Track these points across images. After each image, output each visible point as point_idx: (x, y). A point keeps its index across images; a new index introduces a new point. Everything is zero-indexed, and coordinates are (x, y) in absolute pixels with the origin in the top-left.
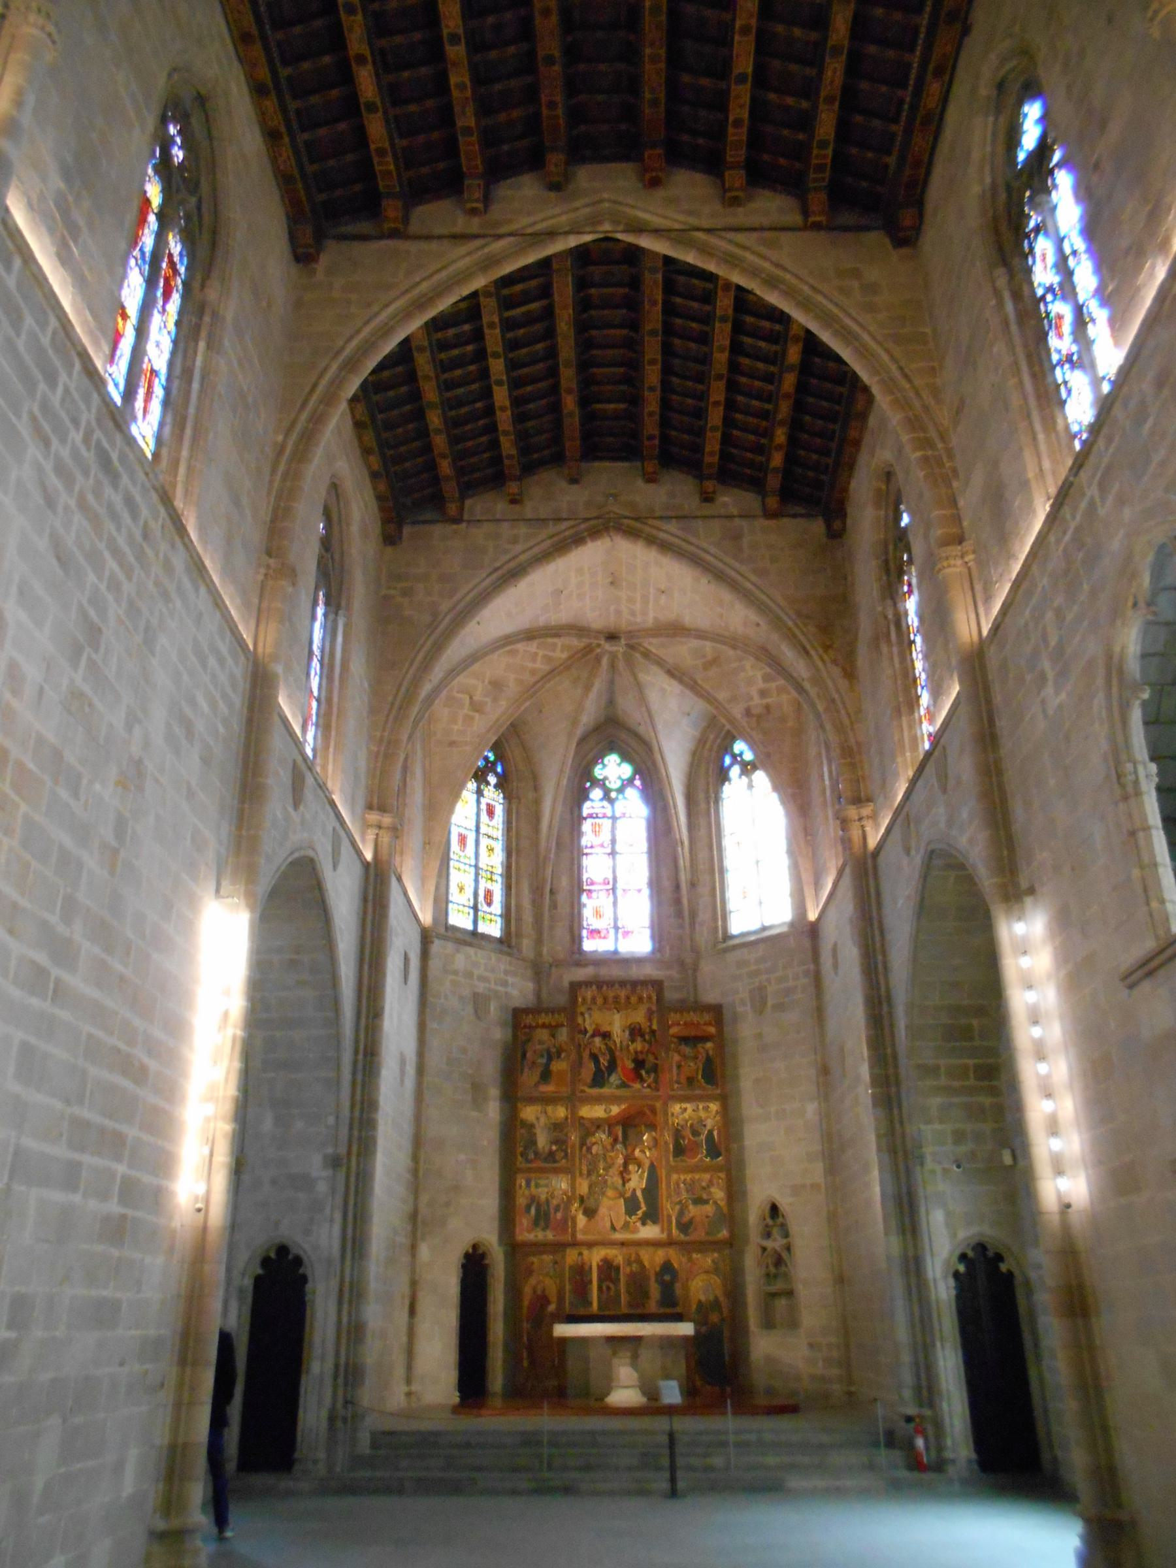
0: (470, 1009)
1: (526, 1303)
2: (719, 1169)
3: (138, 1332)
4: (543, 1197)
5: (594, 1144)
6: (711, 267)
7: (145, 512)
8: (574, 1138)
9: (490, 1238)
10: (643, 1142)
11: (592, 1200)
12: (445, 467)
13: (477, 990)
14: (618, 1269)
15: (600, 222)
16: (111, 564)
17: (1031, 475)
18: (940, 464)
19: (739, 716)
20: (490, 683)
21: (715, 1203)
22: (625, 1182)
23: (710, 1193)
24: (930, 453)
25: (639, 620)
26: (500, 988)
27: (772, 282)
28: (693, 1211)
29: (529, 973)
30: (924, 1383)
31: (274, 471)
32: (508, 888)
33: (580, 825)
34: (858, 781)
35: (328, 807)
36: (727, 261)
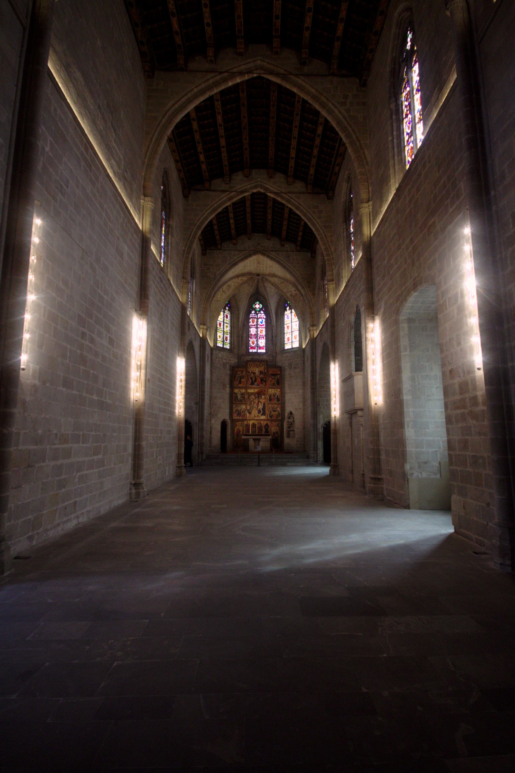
0: (222, 366)
1: (235, 432)
2: (280, 404)
4: (239, 409)
6: (284, 202)
8: (246, 397)
9: (227, 418)
10: (262, 398)
12: (218, 237)
14: (256, 425)
17: (343, 276)
19: (289, 296)
21: (278, 411)
23: (277, 409)
24: (329, 257)
25: (265, 271)
27: (297, 208)
28: (273, 413)
32: (231, 337)
34: (313, 321)
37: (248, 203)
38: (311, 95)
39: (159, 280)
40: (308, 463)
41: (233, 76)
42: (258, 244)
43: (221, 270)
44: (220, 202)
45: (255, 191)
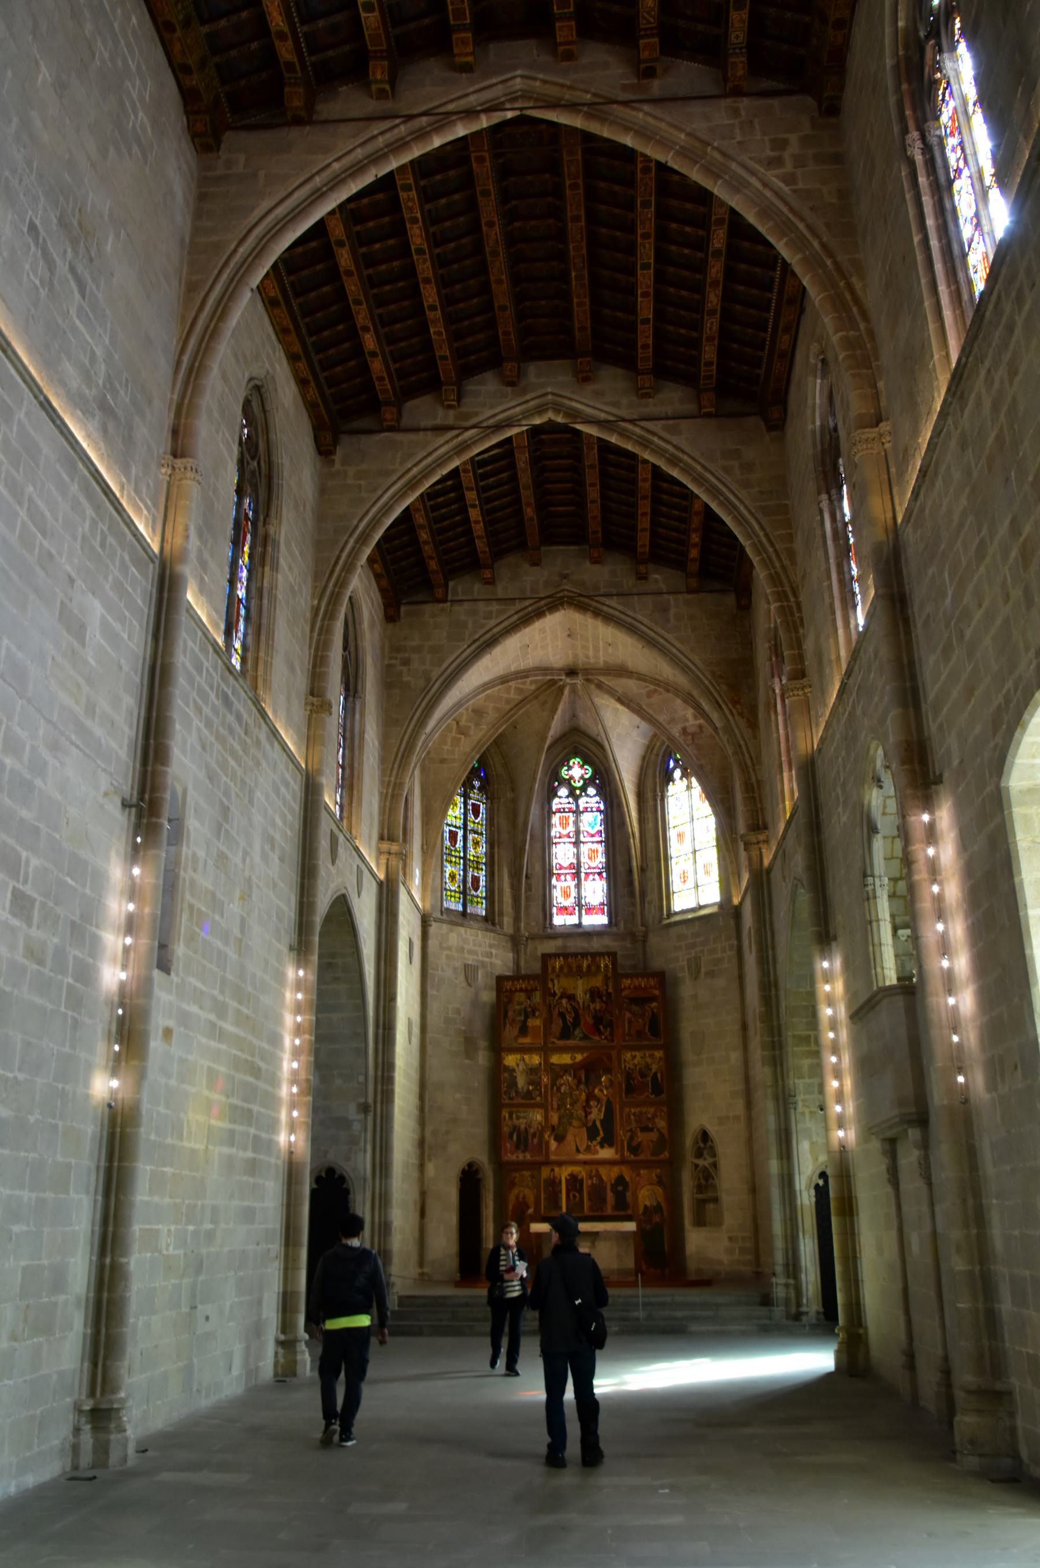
0: (462, 978)
1: (511, 1207)
3: (263, 1226)
4: (523, 1127)
5: (562, 1085)
6: (629, 447)
7: (245, 716)
9: (483, 1158)
10: (600, 1083)
11: (561, 1128)
12: (433, 565)
13: (467, 962)
14: (582, 1181)
15: (546, 410)
16: (232, 763)
18: (792, 614)
20: (473, 711)
21: (658, 1130)
22: (587, 1114)
25: (592, 661)
26: (486, 959)
27: (674, 461)
28: (641, 1137)
29: (509, 945)
30: (791, 1262)
31: (312, 631)
33: (550, 819)
35: (354, 853)
36: (641, 444)
37: (522, 460)
38: (678, 147)
39: (218, 703)
40: (767, 1322)
41: (443, 120)
42: (565, 577)
43: (445, 665)
44: (430, 460)
45: (537, 421)
